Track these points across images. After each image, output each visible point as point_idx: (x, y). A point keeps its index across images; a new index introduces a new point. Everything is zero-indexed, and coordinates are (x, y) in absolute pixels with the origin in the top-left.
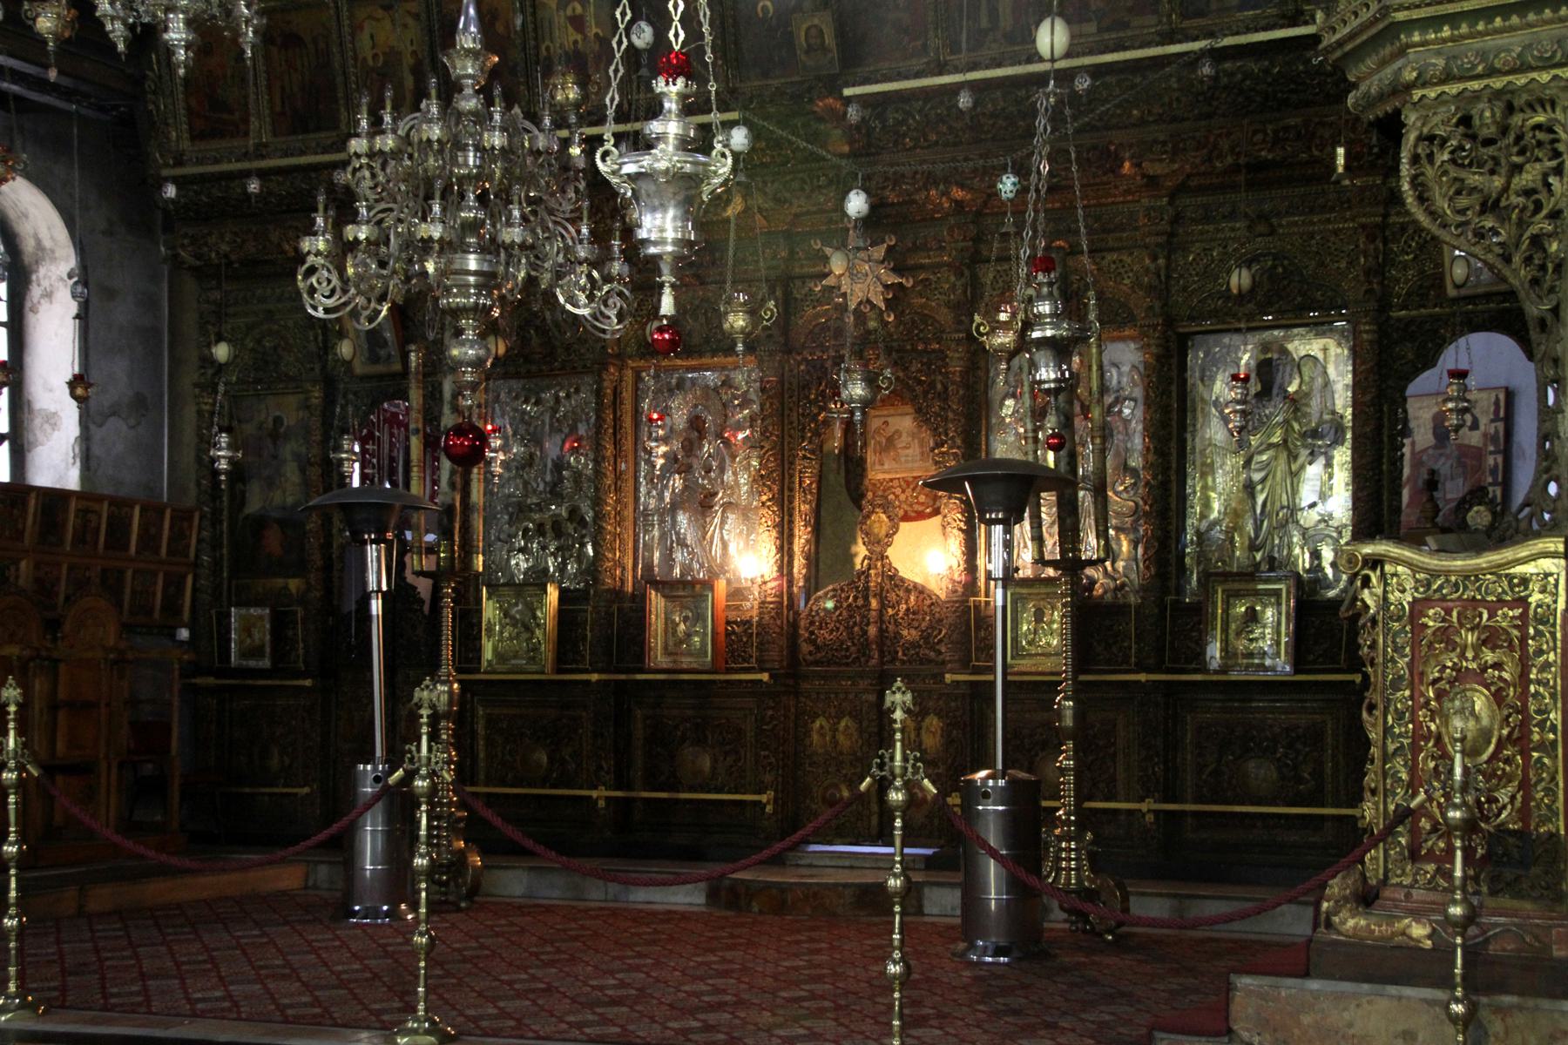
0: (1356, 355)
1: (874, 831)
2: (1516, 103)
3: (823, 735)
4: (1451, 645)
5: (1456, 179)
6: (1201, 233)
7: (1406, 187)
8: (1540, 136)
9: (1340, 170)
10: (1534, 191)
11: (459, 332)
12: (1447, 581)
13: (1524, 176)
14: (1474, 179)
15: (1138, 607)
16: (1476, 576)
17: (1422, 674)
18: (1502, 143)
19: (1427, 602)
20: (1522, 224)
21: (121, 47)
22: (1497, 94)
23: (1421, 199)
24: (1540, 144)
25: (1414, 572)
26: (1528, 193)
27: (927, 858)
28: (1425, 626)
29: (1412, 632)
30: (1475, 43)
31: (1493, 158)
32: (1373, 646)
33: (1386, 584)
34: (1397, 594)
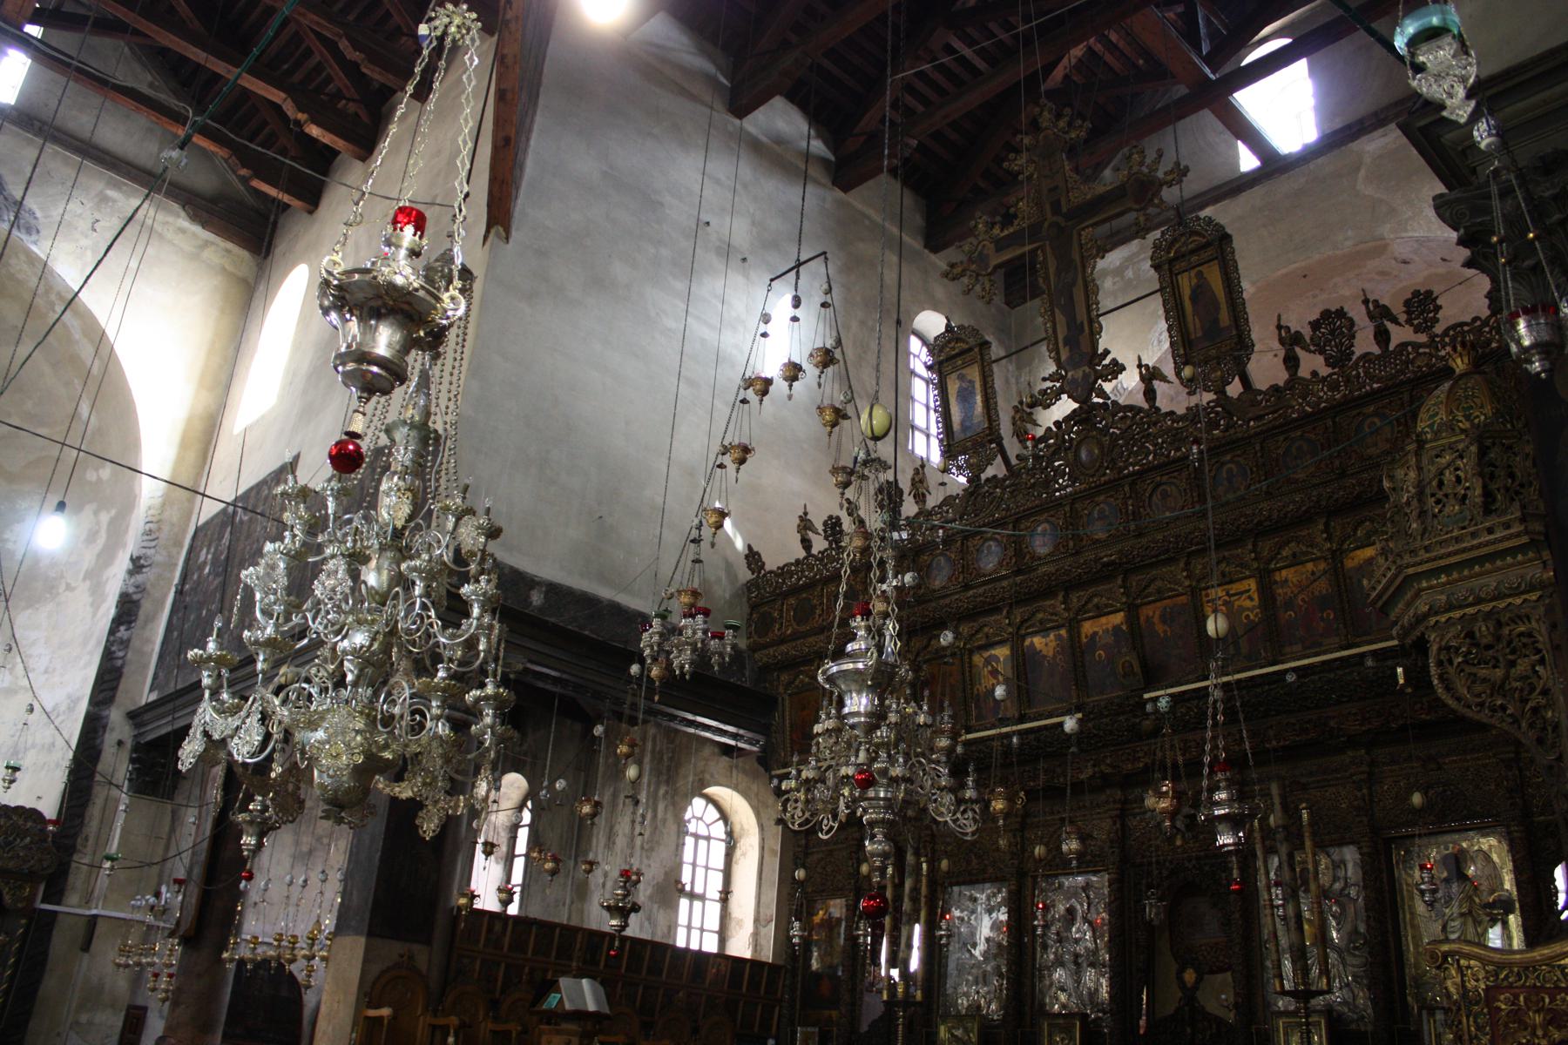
0: (1513, 849)
2: (1505, 618)
5: (1470, 674)
7: (1436, 682)
8: (1524, 640)
9: (1401, 681)
10: (1528, 677)
11: (873, 836)
12: (1511, 972)
13: (1519, 667)
14: (1483, 672)
20: (1527, 701)
22: (1489, 614)
23: (1448, 689)
24: (1525, 645)
25: (1484, 966)
26: (1523, 678)
29: (1489, 1013)
31: (1494, 658)
33: (1463, 975)
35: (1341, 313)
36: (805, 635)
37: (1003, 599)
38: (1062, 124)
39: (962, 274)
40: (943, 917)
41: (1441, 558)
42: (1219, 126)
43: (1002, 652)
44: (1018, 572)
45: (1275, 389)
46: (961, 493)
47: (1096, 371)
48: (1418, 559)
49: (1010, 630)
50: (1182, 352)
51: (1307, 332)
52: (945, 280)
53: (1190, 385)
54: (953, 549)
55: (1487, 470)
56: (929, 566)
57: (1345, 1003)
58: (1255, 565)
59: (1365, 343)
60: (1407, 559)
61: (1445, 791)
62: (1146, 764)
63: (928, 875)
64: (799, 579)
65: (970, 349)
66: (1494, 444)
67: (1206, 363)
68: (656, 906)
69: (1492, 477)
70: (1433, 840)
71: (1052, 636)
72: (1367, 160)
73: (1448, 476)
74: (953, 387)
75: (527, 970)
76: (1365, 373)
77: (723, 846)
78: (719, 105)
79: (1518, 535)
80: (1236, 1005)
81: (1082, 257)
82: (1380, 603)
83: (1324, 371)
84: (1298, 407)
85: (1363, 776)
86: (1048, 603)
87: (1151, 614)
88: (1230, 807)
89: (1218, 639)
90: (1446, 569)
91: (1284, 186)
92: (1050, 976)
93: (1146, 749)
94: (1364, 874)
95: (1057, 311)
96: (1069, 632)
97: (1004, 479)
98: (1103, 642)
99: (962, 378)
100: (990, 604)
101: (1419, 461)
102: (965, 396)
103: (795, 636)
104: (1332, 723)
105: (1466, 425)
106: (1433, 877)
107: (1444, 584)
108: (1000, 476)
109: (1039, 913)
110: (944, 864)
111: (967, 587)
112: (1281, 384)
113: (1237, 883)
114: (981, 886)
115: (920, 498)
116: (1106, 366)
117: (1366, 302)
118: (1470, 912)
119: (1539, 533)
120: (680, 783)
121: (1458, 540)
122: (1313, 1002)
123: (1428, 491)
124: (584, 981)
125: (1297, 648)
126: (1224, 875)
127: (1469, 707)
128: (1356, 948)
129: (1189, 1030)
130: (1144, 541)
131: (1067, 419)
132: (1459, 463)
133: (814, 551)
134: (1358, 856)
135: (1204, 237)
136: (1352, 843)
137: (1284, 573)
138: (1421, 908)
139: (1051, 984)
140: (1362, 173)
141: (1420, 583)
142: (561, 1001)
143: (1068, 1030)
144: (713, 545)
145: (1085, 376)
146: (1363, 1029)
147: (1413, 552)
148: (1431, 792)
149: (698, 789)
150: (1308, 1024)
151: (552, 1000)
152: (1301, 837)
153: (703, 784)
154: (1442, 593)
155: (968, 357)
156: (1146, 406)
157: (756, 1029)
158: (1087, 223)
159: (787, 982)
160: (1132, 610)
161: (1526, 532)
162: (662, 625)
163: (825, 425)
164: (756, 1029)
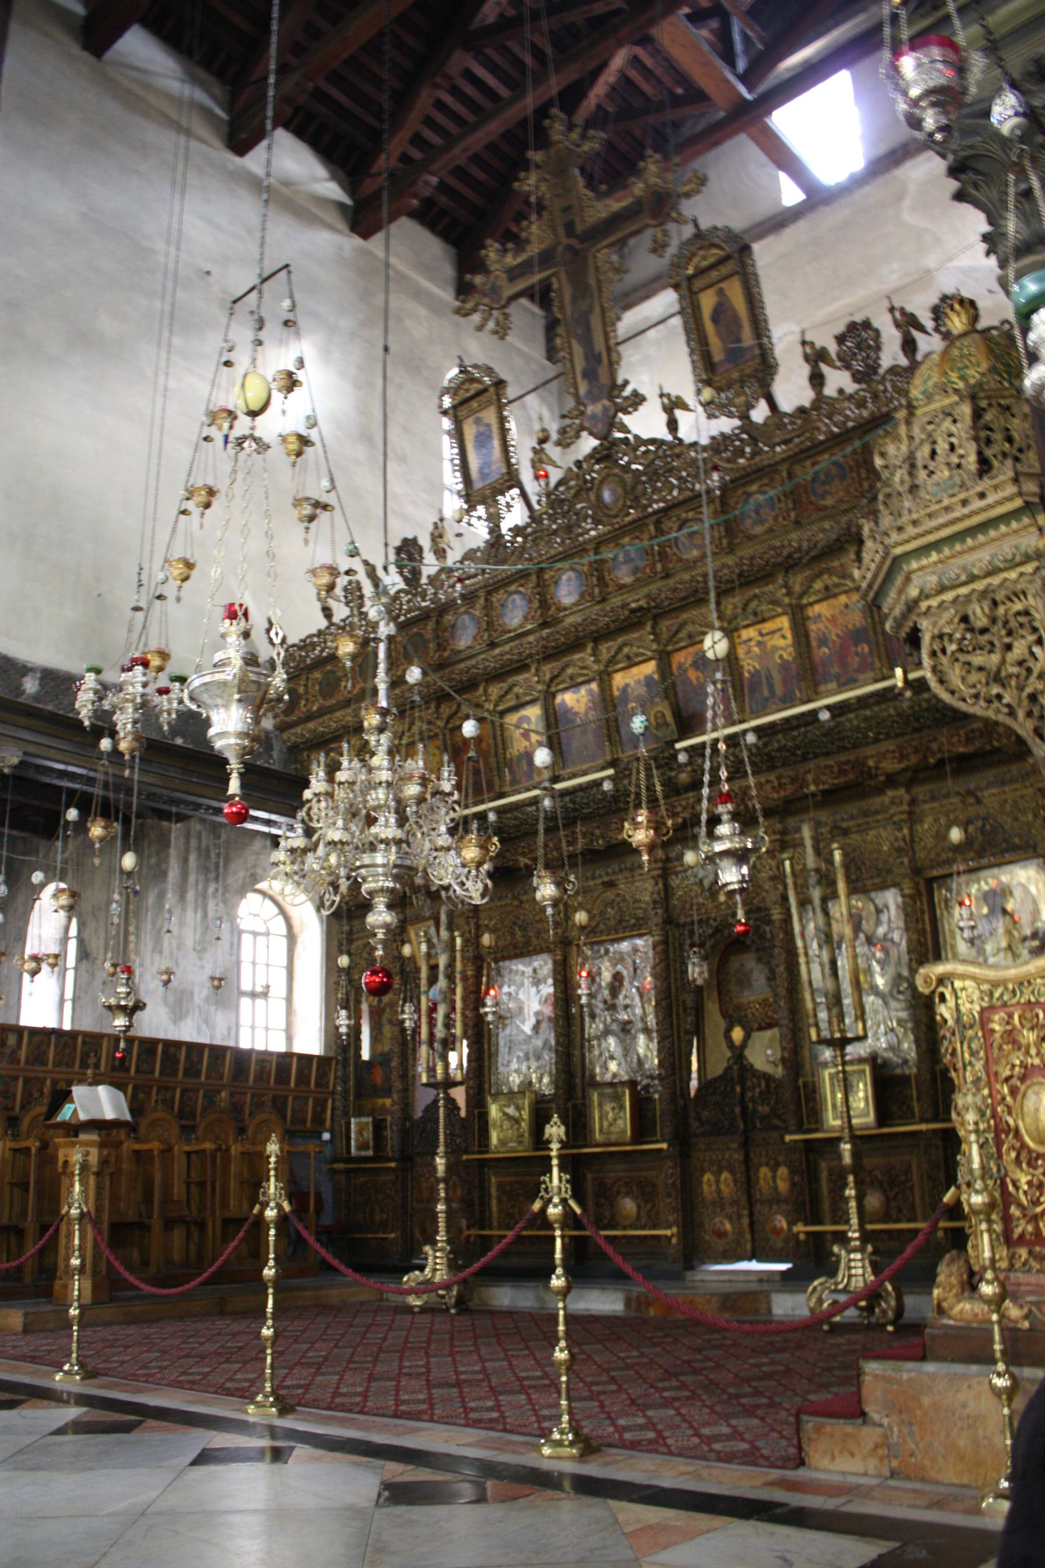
1: (749, 1254)
2: (999, 597)
3: (710, 1186)
4: (1017, 1045)
6: (932, 809)
8: (1021, 619)
12: (1006, 989)
14: (977, 659)
15: (916, 1076)
16: (1029, 982)
17: (996, 1074)
18: (994, 629)
19: (992, 1008)
20: (1021, 688)
21: (87, 723)
22: (984, 594)
23: (941, 682)
24: (1021, 625)
25: (978, 985)
26: (1020, 663)
27: (782, 1273)
28: (993, 1031)
29: (984, 1036)
30: (960, 561)
32: (954, 1053)
33: (957, 998)
34: (968, 1005)
35: (867, 325)
36: (331, 710)
37: (530, 656)
38: (574, 136)
39: (474, 310)
40: (487, 993)
41: (930, 532)
42: (763, 158)
43: (534, 713)
44: (544, 625)
45: (801, 410)
46: (482, 545)
47: (616, 404)
48: (905, 536)
49: (540, 687)
50: (704, 377)
51: (833, 348)
52: (457, 318)
53: (712, 409)
54: (478, 606)
55: (983, 434)
56: (453, 626)
57: (891, 1048)
58: (787, 600)
59: (891, 355)
60: (895, 537)
61: (984, 825)
62: (685, 819)
63: (462, 950)
64: (322, 651)
65: (485, 390)
66: (990, 405)
67: (729, 387)
68: (213, 1008)
69: (989, 442)
70: (973, 876)
71: (583, 690)
72: (912, 187)
73: (942, 446)
74: (470, 431)
75: (48, 1082)
76: (894, 386)
77: (284, 943)
78: (217, 143)
79: (1010, 499)
80: (783, 1060)
81: (599, 281)
82: (871, 595)
83: (851, 387)
84: (826, 427)
85: (904, 817)
86: (577, 656)
87: (682, 660)
88: (731, 841)
89: (717, 660)
90: (936, 546)
91: (828, 218)
92: (599, 1045)
93: (684, 803)
94: (906, 915)
95: (574, 342)
96: (600, 686)
97: (525, 528)
98: (636, 693)
99: (478, 421)
100: (518, 661)
101: (909, 430)
102: (482, 440)
103: (322, 712)
104: (871, 763)
105: (961, 385)
106: (971, 914)
107: (935, 563)
108: (520, 523)
109: (583, 983)
110: (486, 939)
111: (492, 645)
112: (807, 404)
113: (742, 924)
114: (527, 959)
115: (440, 553)
116: (626, 398)
117: (892, 310)
118: (1010, 947)
119: (1034, 494)
120: (230, 880)
121: (948, 509)
122: (849, 1049)
123: (919, 463)
124: (102, 1090)
125: (833, 686)
126: (768, 929)
127: (964, 700)
128: (899, 992)
129: (738, 1089)
130: (671, 582)
131: (590, 457)
132: (953, 429)
133: (336, 619)
134: (900, 899)
135: (721, 248)
136: (895, 885)
137: (817, 608)
138: (962, 947)
139: (601, 1054)
140: (907, 202)
141: (909, 563)
142: (75, 1111)
143: (618, 1098)
144: (178, 600)
145: (606, 409)
146: (907, 1072)
147: (900, 529)
148: (971, 828)
149: (250, 884)
150: (844, 1072)
151: (66, 1113)
152: (833, 883)
153: (255, 879)
154: (933, 573)
155: (483, 398)
156: (669, 438)
157: (309, 1124)
158: (599, 246)
159: (339, 1073)
160: (664, 658)
161: (1020, 494)
162: (97, 681)
163: (288, 455)
164: (309, 1124)
